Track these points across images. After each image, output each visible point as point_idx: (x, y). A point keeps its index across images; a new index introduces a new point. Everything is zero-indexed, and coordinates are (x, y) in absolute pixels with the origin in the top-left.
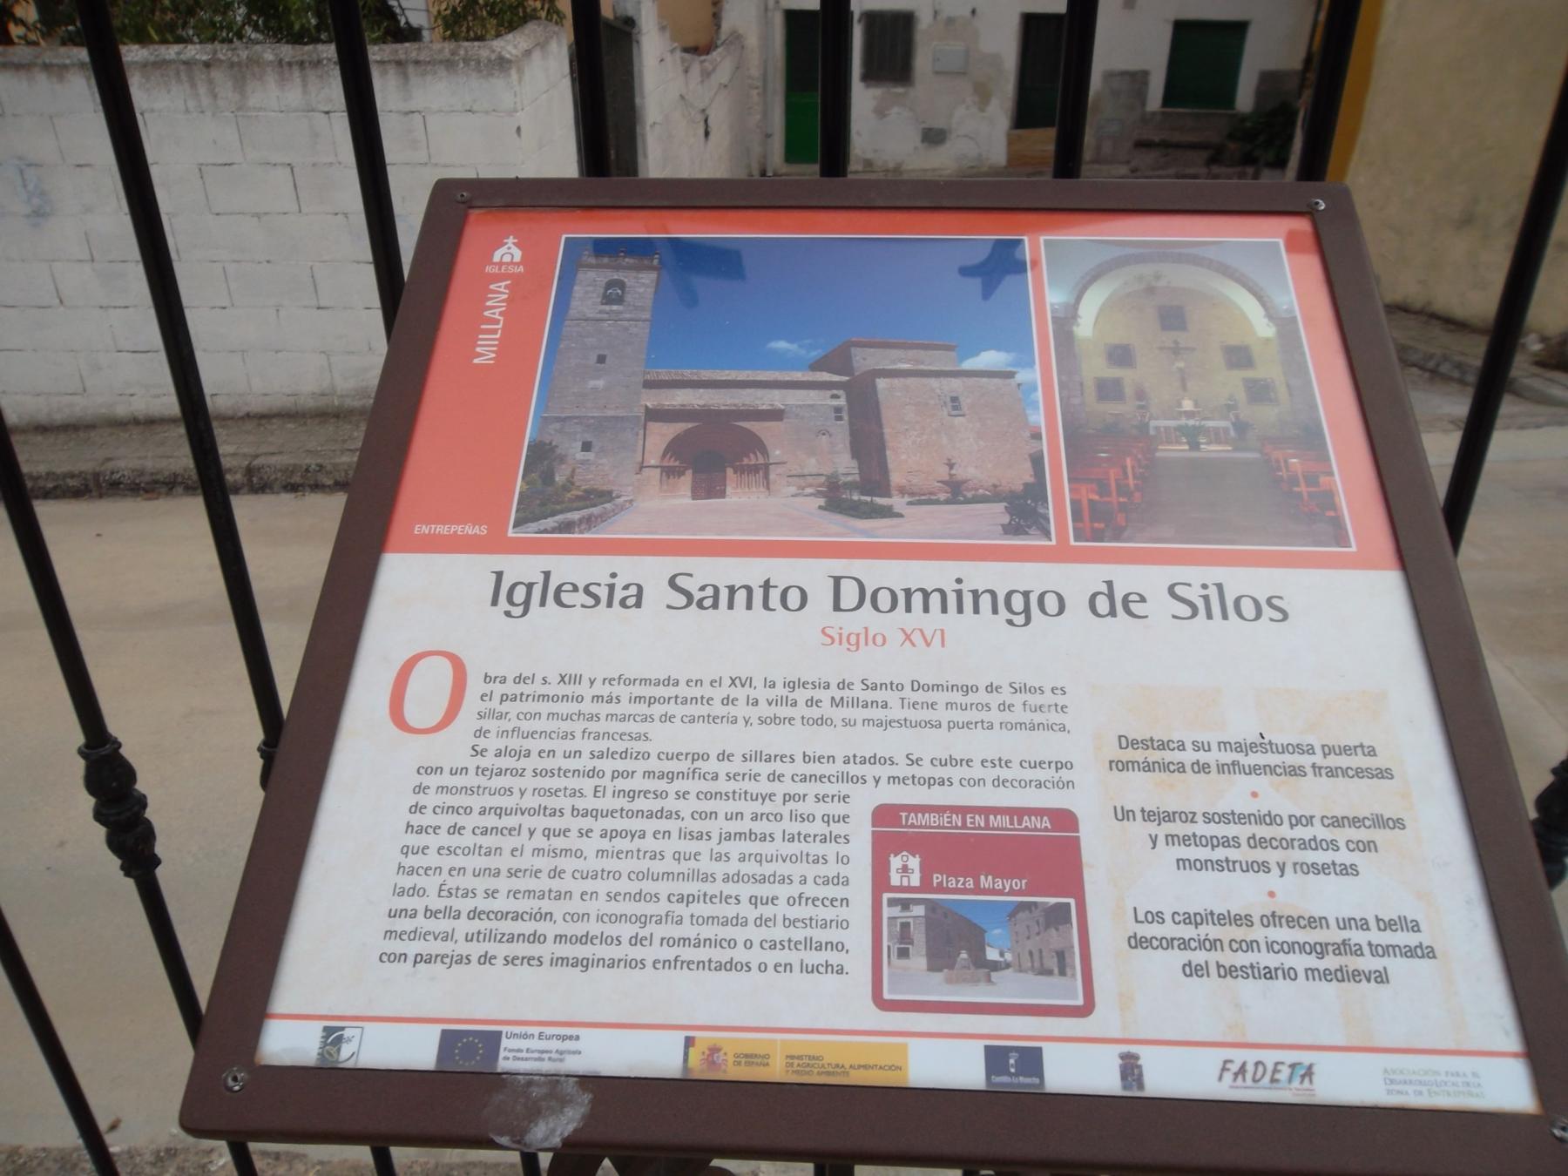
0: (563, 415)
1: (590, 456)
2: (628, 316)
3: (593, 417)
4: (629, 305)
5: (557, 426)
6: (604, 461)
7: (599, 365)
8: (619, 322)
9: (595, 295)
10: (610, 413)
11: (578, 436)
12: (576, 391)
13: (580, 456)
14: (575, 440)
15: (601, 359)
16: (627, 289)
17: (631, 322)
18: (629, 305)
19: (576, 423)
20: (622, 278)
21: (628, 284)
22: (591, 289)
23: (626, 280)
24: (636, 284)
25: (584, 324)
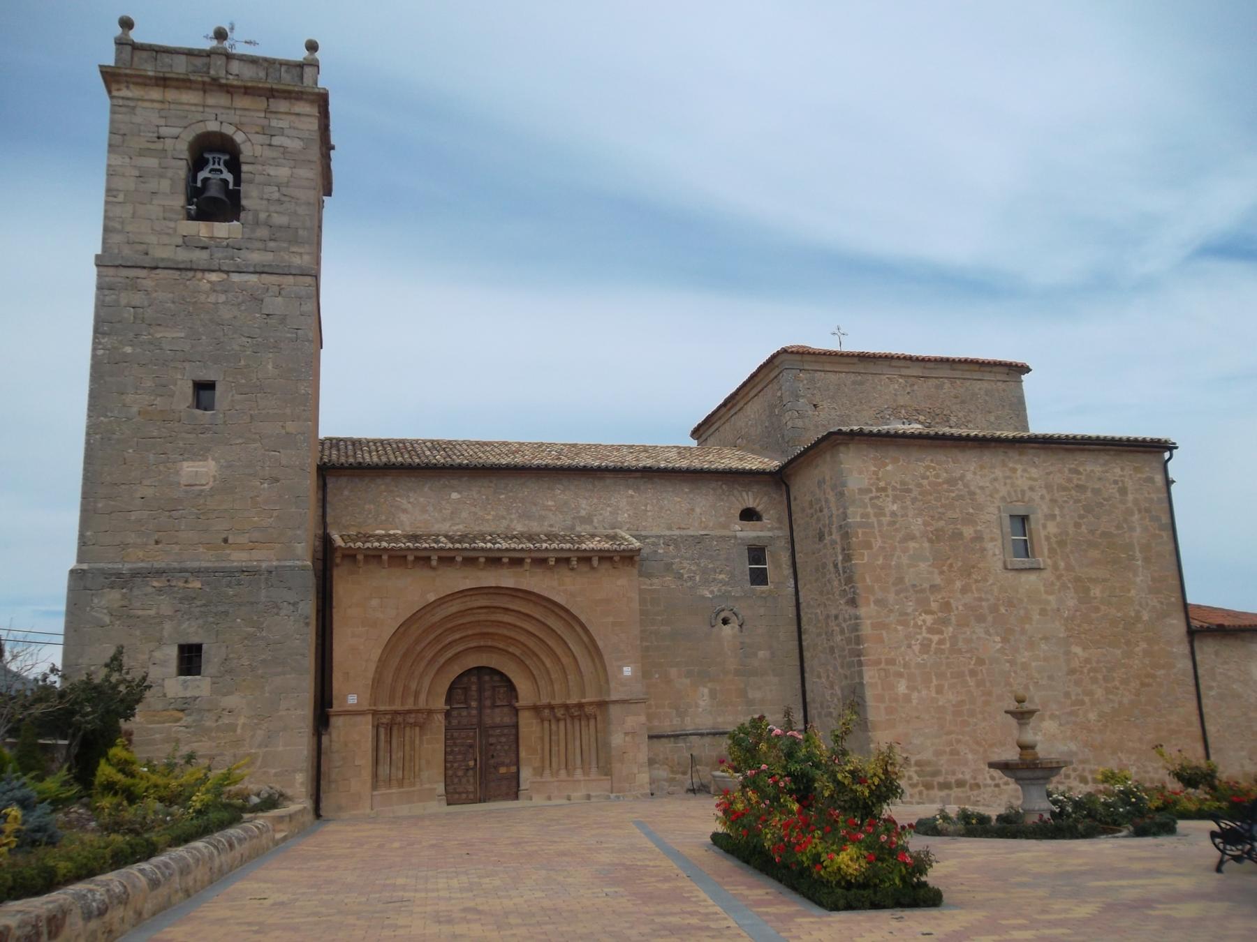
0: (126, 567)
1: (199, 686)
2: (256, 257)
3: (197, 572)
4: (257, 223)
5: (113, 597)
6: (232, 701)
7: (199, 412)
8: (235, 278)
9: (165, 185)
10: (238, 558)
11: (168, 627)
12: (149, 492)
13: (175, 686)
14: (160, 642)
15: (203, 389)
16: (244, 168)
17: (266, 278)
18: (257, 223)
19: (160, 591)
20: (228, 130)
21: (246, 151)
22: (151, 162)
23: (239, 138)
24: (268, 153)
25: (148, 280)
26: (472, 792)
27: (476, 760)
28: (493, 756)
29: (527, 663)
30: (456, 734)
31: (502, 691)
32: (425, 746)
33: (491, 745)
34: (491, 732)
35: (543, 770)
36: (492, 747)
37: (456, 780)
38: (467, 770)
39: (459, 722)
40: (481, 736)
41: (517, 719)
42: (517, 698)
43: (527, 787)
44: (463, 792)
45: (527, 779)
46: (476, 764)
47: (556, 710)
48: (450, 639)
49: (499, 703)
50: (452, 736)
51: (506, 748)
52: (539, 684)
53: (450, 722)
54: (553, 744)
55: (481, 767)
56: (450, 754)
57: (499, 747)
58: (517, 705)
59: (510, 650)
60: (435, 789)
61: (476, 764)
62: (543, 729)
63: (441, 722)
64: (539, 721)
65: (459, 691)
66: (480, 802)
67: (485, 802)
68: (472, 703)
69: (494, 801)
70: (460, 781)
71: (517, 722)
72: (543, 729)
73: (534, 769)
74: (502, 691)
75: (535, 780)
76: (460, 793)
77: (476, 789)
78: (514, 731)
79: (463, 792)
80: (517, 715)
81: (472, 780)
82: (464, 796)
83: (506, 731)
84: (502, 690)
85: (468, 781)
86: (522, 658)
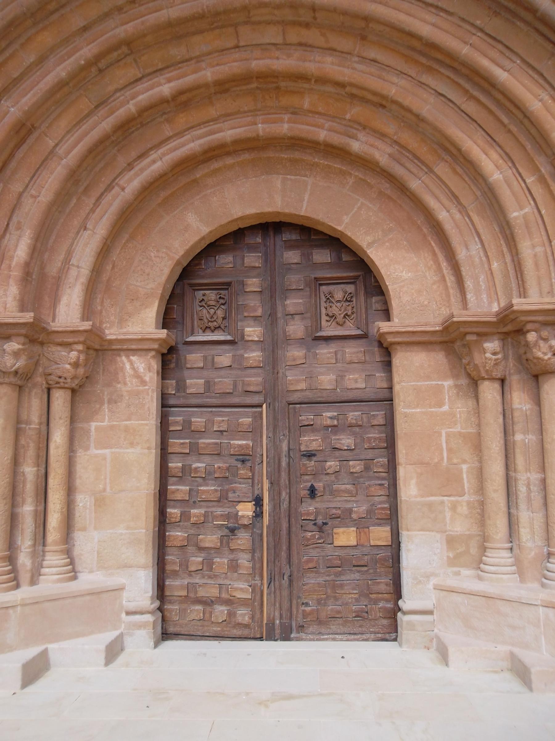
26: (244, 603)
27: (258, 502)
28: (312, 492)
29: (414, 184)
30: (198, 421)
31: (339, 295)
32: (94, 451)
33: (310, 455)
34: (306, 417)
35: (483, 549)
36: (311, 464)
37: (196, 560)
38: (233, 530)
39: (208, 385)
40: (274, 427)
41: (390, 379)
42: (387, 314)
43: (427, 605)
44: (220, 601)
45: (428, 576)
46: (259, 514)
47: (532, 337)
48: (144, 98)
49: (329, 330)
50: (187, 423)
51: (357, 466)
52: (461, 254)
53: (181, 386)
54: (520, 461)
55: (274, 530)
56: (181, 479)
57: (332, 464)
58: (384, 326)
59: (356, 146)
60: (121, 589)
61: (259, 514)
62: (478, 411)
63: (143, 382)
64: (464, 381)
65: (212, 295)
66: (271, 637)
67: (286, 637)
68: (248, 330)
69: (318, 636)
70: (209, 564)
71: (391, 388)
72: (478, 411)
73: (451, 541)
74: (339, 295)
75: (452, 582)
76: (208, 603)
77: (256, 590)
78: (379, 418)
79: (220, 601)
80: (388, 365)
81: (244, 560)
82: (221, 611)
83: (353, 415)
84: (338, 292)
85: (234, 566)
86: (398, 171)
